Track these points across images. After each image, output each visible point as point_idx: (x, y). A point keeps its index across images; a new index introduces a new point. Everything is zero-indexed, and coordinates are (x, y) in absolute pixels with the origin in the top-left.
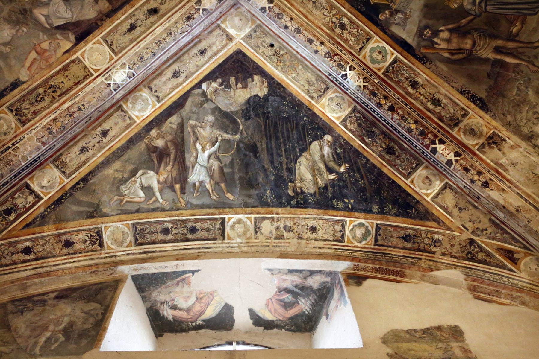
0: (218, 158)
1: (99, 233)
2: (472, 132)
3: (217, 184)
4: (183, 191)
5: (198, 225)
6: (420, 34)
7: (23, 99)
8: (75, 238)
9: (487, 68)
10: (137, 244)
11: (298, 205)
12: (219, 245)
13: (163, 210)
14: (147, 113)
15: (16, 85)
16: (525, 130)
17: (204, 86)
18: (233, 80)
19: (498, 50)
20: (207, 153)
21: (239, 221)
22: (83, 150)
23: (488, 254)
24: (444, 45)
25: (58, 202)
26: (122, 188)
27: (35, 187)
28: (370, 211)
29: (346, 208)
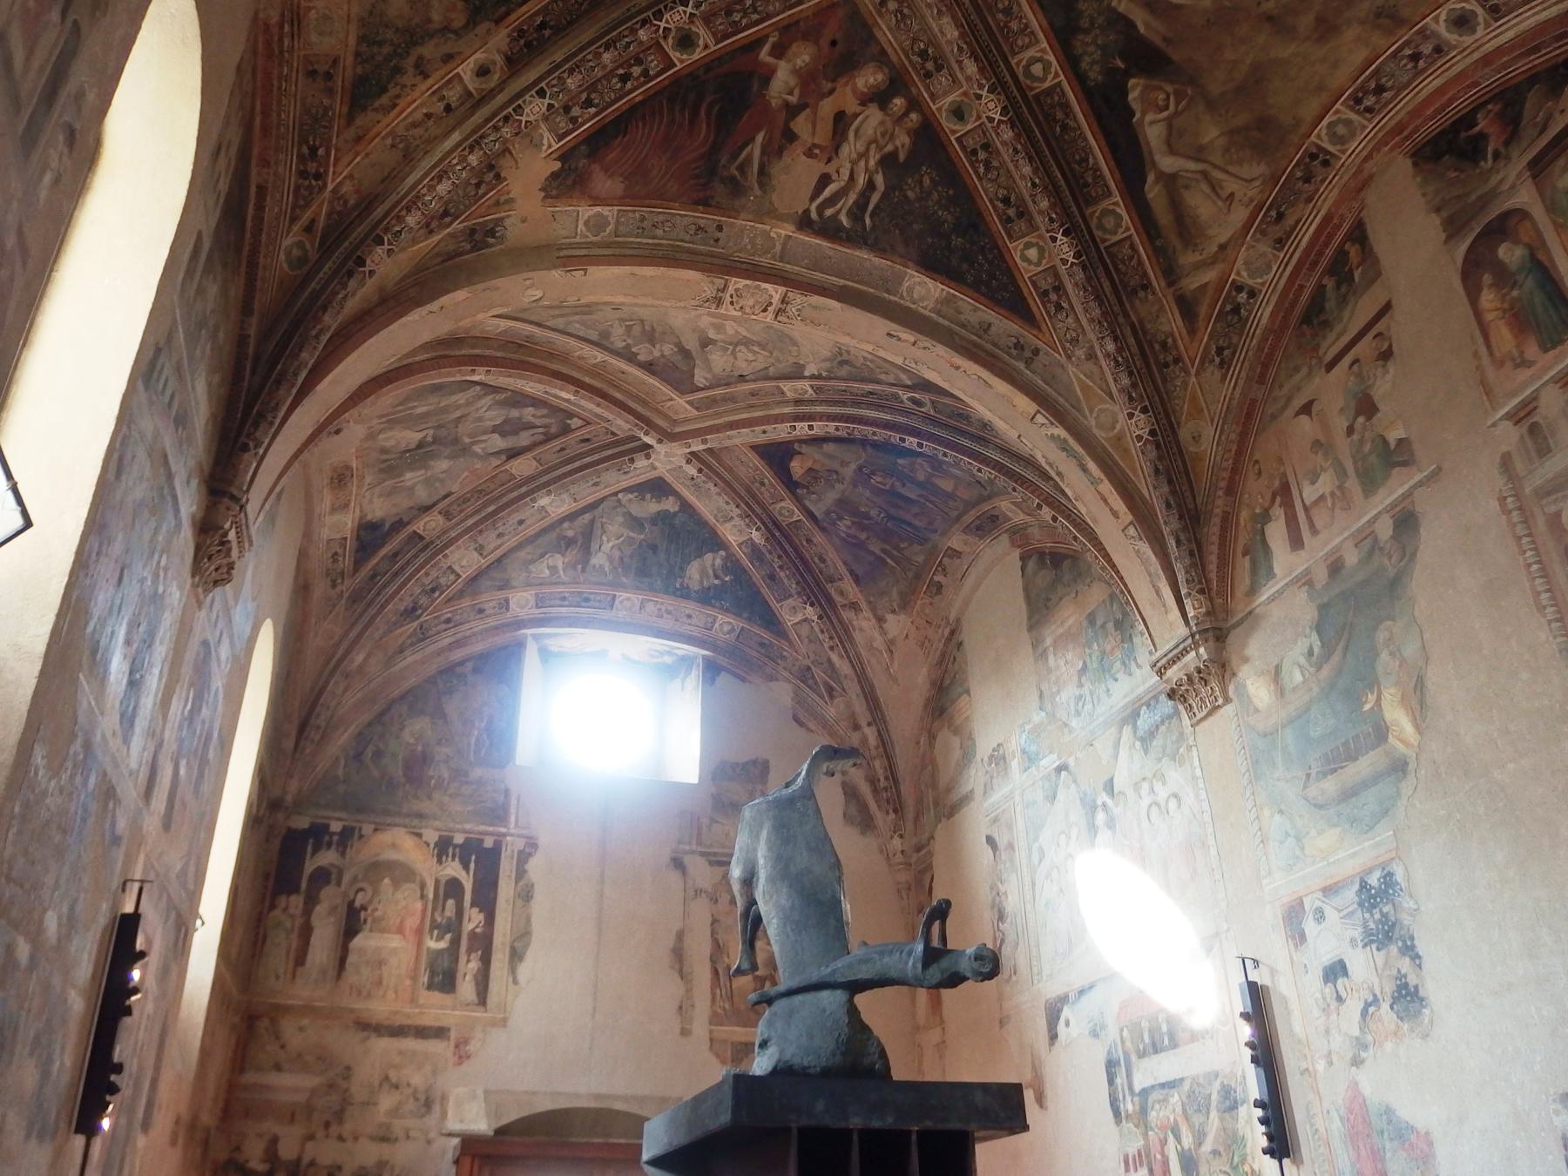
0: (620, 549)
1: (507, 601)
2: (841, 593)
3: (615, 568)
4: (583, 570)
5: (592, 597)
6: (828, 513)
7: (451, 504)
8: (486, 606)
9: (872, 558)
10: (537, 607)
11: (682, 597)
12: (606, 615)
13: (564, 583)
14: (563, 509)
15: (446, 497)
16: (880, 613)
17: (620, 495)
18: (648, 496)
19: (883, 550)
20: (611, 544)
21: (628, 599)
22: (500, 535)
23: (816, 683)
24: (843, 528)
25: (474, 579)
26: (532, 568)
27: (456, 568)
28: (740, 616)
29: (721, 608)
